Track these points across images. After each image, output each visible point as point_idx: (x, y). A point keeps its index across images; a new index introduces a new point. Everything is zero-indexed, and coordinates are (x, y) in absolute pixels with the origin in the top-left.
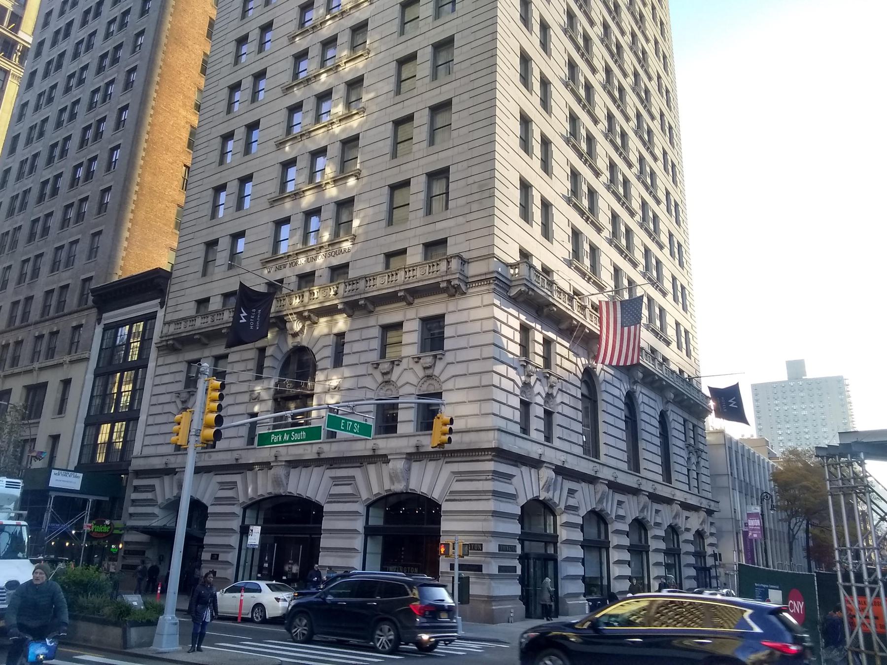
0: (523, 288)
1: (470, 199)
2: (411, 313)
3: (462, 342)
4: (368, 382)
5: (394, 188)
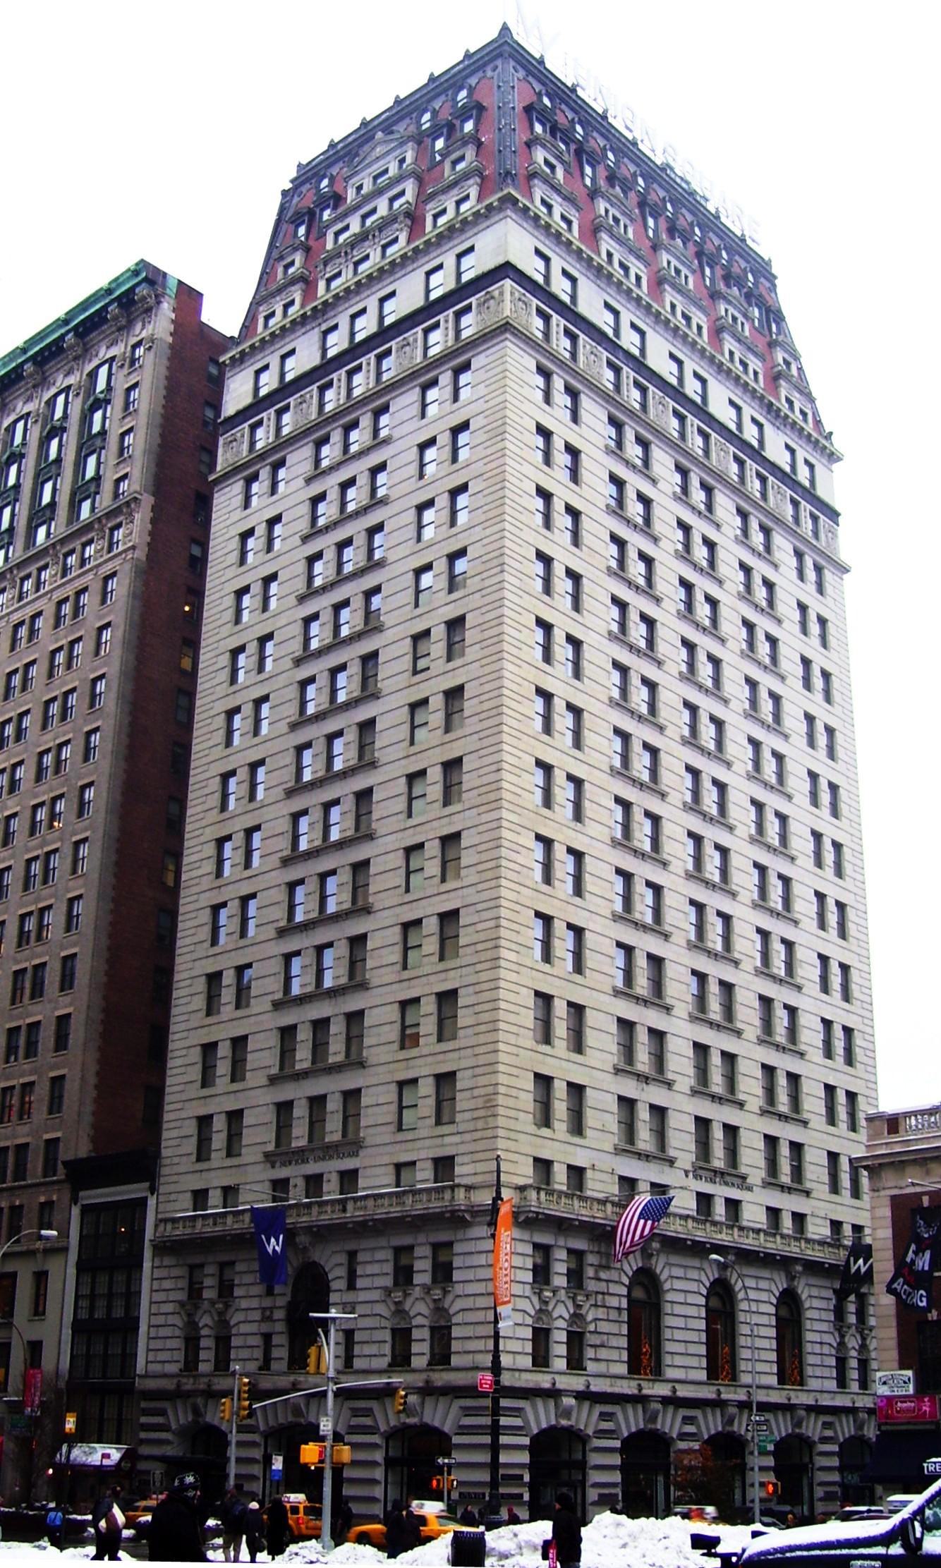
0: (531, 1215)
1: (476, 1114)
2: (422, 1238)
3: (470, 1275)
4: (381, 1309)
5: (401, 1084)
